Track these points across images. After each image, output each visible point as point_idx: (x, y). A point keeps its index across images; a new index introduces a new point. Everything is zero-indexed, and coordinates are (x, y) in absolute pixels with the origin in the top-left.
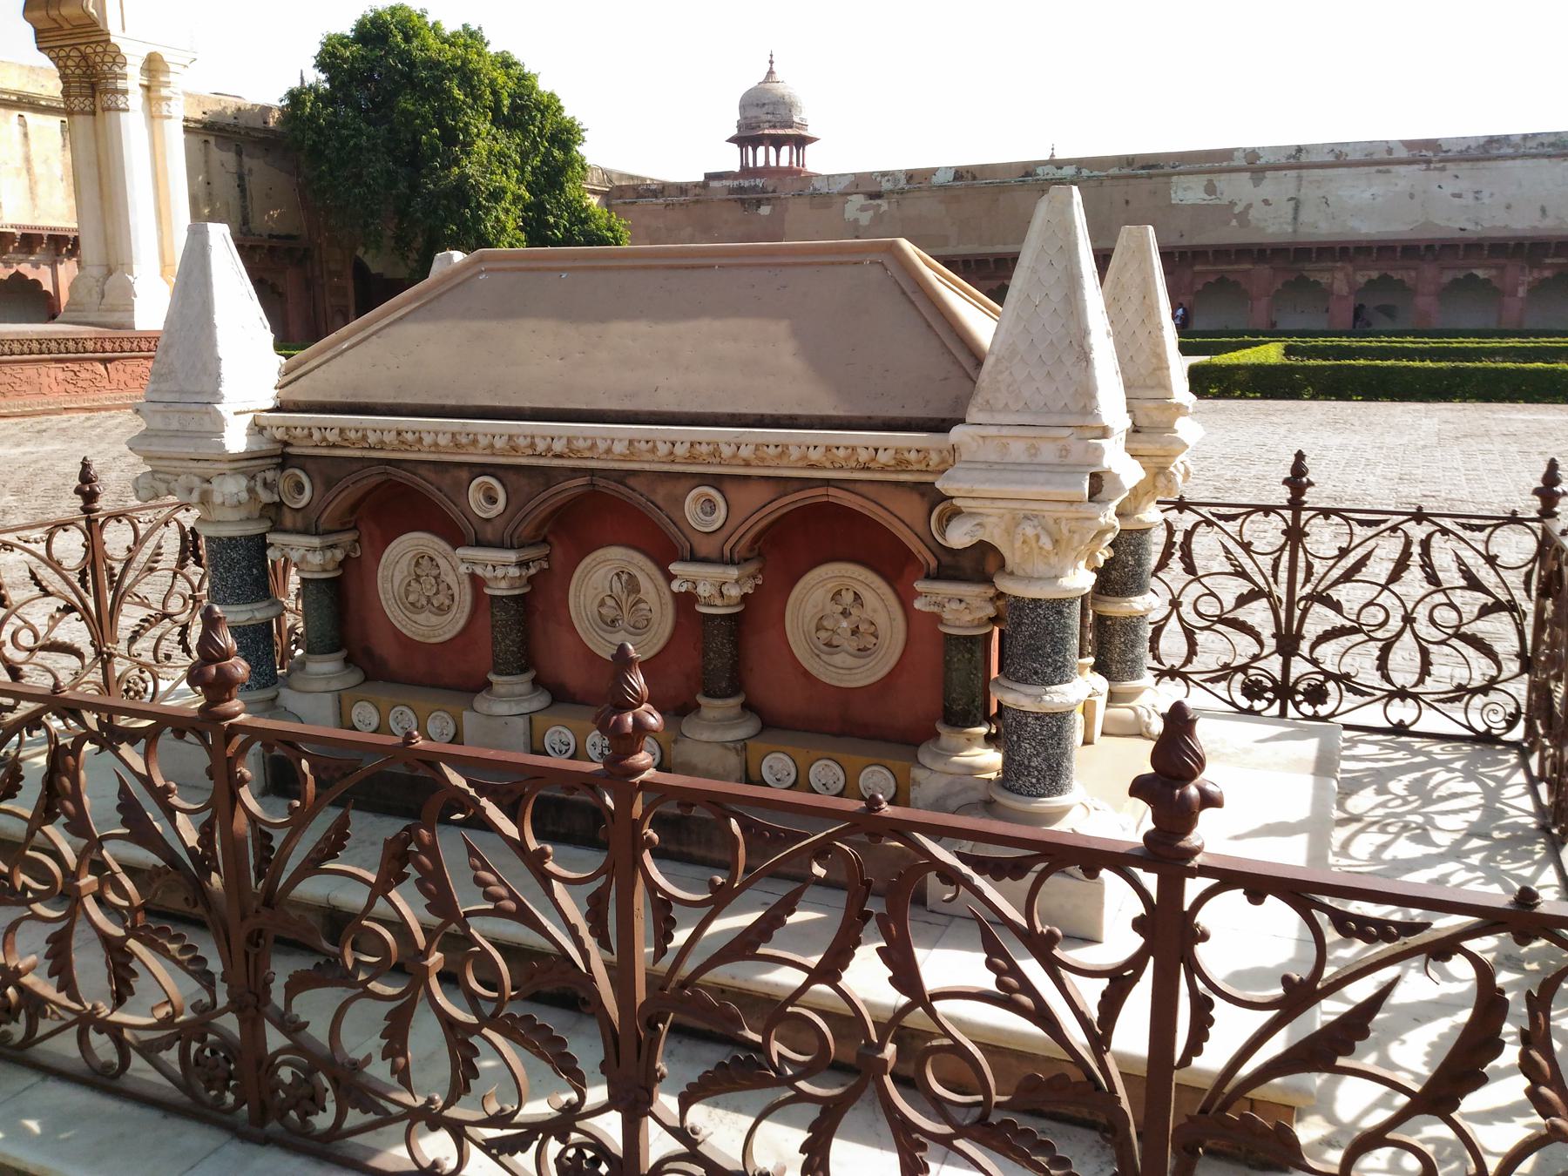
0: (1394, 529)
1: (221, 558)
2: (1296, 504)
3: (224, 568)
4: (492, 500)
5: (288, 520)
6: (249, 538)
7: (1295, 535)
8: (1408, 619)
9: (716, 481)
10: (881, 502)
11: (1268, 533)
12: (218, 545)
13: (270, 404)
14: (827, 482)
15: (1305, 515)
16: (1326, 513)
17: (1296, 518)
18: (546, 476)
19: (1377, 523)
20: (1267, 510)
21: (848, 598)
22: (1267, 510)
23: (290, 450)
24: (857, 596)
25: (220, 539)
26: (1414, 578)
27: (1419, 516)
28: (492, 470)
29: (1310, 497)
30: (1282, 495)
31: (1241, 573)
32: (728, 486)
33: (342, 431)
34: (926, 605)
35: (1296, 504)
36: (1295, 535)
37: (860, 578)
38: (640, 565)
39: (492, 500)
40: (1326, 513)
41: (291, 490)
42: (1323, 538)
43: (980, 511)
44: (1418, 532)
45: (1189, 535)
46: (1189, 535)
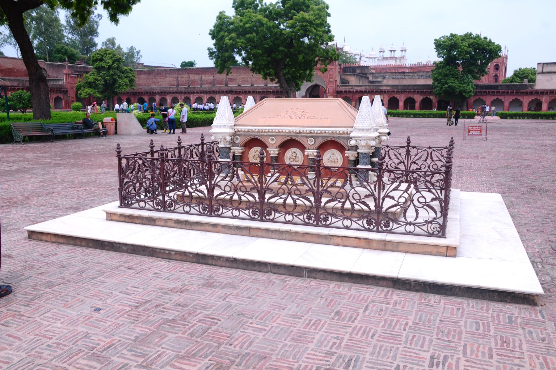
0: (425, 150)
2: (408, 146)
7: (408, 152)
8: (429, 167)
11: (403, 151)
15: (410, 148)
16: (414, 147)
17: (408, 148)
19: (421, 149)
20: (403, 147)
22: (403, 147)
26: (429, 160)
27: (430, 148)
29: (411, 144)
30: (406, 144)
31: (398, 158)
35: (408, 146)
36: (408, 152)
38: (298, 151)
40: (414, 147)
42: (413, 152)
44: (430, 151)
45: (388, 152)
46: (388, 152)
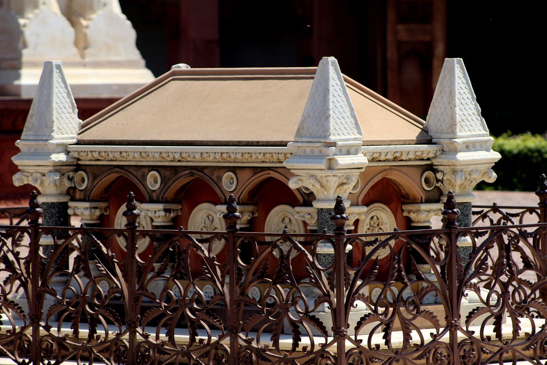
1: (48, 212)
3: (49, 217)
4: (156, 182)
5: (78, 195)
6: (60, 204)
9: (233, 169)
10: (286, 175)
12: (47, 206)
13: (75, 141)
14: (269, 168)
18: (175, 170)
21: (287, 220)
23: (80, 162)
24: (290, 220)
25: (48, 203)
28: (156, 168)
32: (238, 172)
33: (100, 152)
34: (299, 217)
37: (289, 211)
39: (156, 182)
41: (80, 181)
43: (299, 174)
